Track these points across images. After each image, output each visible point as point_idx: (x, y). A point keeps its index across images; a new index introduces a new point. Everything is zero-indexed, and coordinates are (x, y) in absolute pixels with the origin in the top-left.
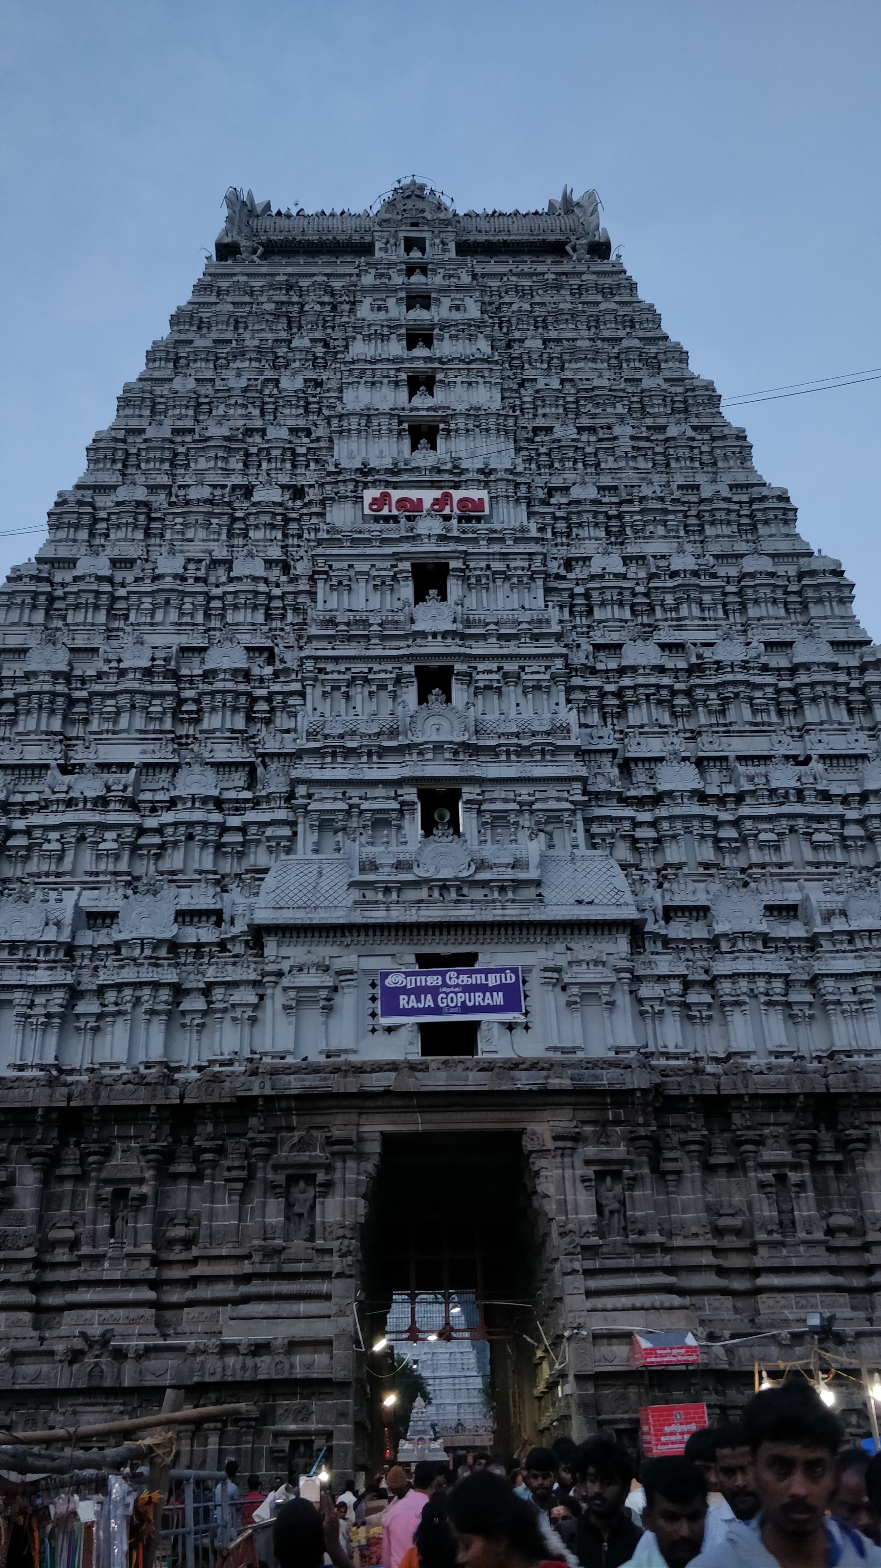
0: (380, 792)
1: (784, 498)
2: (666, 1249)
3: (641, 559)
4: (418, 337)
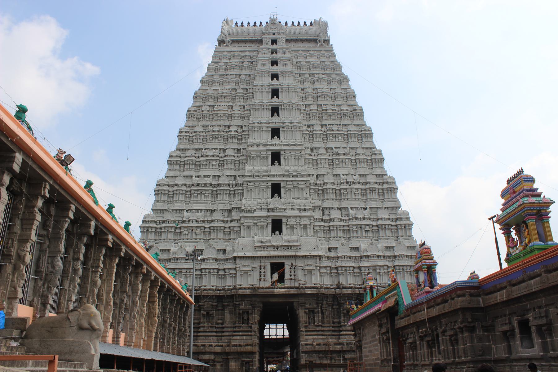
0: (262, 220)
1: (370, 130)
2: (322, 326)
3: (331, 148)
4: (275, 76)
